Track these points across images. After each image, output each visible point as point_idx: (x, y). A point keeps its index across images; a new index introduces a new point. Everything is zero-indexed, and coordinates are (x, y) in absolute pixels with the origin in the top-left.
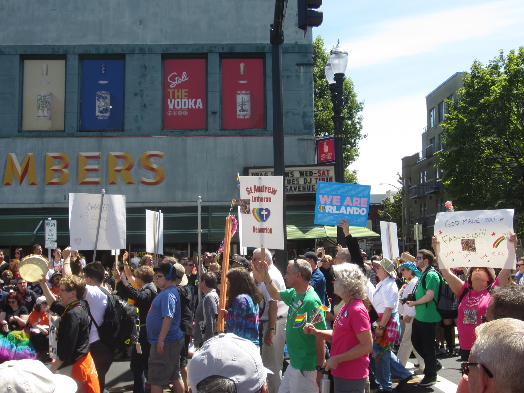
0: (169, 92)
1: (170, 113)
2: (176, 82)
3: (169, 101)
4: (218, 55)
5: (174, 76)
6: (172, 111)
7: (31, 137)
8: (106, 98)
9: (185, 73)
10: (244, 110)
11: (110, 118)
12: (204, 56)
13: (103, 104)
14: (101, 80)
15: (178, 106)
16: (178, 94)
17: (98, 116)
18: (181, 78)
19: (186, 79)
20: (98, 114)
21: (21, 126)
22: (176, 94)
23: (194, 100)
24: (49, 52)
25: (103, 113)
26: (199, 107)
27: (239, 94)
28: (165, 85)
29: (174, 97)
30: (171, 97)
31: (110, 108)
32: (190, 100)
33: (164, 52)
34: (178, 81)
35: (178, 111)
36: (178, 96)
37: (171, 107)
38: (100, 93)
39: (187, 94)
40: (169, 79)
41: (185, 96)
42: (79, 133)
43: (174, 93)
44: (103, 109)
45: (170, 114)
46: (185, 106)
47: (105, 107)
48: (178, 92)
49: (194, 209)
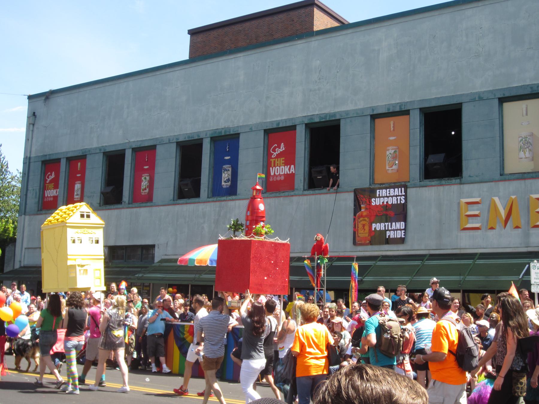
0: (271, 162)
1: (271, 179)
2: (277, 152)
3: (271, 168)
4: (498, 99)
5: (275, 148)
6: (273, 177)
7: (272, 197)
8: (229, 170)
9: (283, 144)
10: (77, 195)
11: (231, 186)
12: (293, 128)
13: (227, 175)
14: (226, 156)
15: (277, 173)
16: (278, 162)
17: (223, 185)
18: (280, 148)
19: (284, 149)
20: (223, 183)
21: (373, 179)
22: (276, 162)
23: (289, 166)
24: (398, 109)
25: (226, 183)
26: (292, 172)
27: (76, 184)
28: (269, 155)
29: (274, 166)
30: (273, 165)
31: (398, 163)
32: (286, 167)
33: (213, 136)
34: (279, 151)
35: (277, 177)
36: (278, 164)
37: (272, 174)
38: (225, 167)
39: (284, 162)
40: (272, 151)
41: (283, 163)
42: (209, 199)
43: (275, 162)
44: (227, 180)
45: (271, 180)
46: (282, 172)
47: (228, 178)
48: (278, 161)
49: (303, 259)
